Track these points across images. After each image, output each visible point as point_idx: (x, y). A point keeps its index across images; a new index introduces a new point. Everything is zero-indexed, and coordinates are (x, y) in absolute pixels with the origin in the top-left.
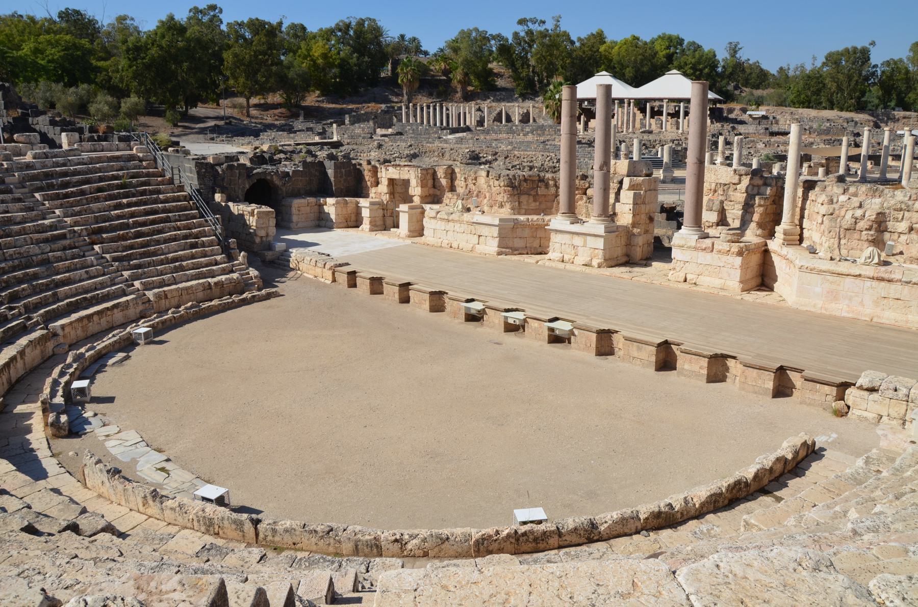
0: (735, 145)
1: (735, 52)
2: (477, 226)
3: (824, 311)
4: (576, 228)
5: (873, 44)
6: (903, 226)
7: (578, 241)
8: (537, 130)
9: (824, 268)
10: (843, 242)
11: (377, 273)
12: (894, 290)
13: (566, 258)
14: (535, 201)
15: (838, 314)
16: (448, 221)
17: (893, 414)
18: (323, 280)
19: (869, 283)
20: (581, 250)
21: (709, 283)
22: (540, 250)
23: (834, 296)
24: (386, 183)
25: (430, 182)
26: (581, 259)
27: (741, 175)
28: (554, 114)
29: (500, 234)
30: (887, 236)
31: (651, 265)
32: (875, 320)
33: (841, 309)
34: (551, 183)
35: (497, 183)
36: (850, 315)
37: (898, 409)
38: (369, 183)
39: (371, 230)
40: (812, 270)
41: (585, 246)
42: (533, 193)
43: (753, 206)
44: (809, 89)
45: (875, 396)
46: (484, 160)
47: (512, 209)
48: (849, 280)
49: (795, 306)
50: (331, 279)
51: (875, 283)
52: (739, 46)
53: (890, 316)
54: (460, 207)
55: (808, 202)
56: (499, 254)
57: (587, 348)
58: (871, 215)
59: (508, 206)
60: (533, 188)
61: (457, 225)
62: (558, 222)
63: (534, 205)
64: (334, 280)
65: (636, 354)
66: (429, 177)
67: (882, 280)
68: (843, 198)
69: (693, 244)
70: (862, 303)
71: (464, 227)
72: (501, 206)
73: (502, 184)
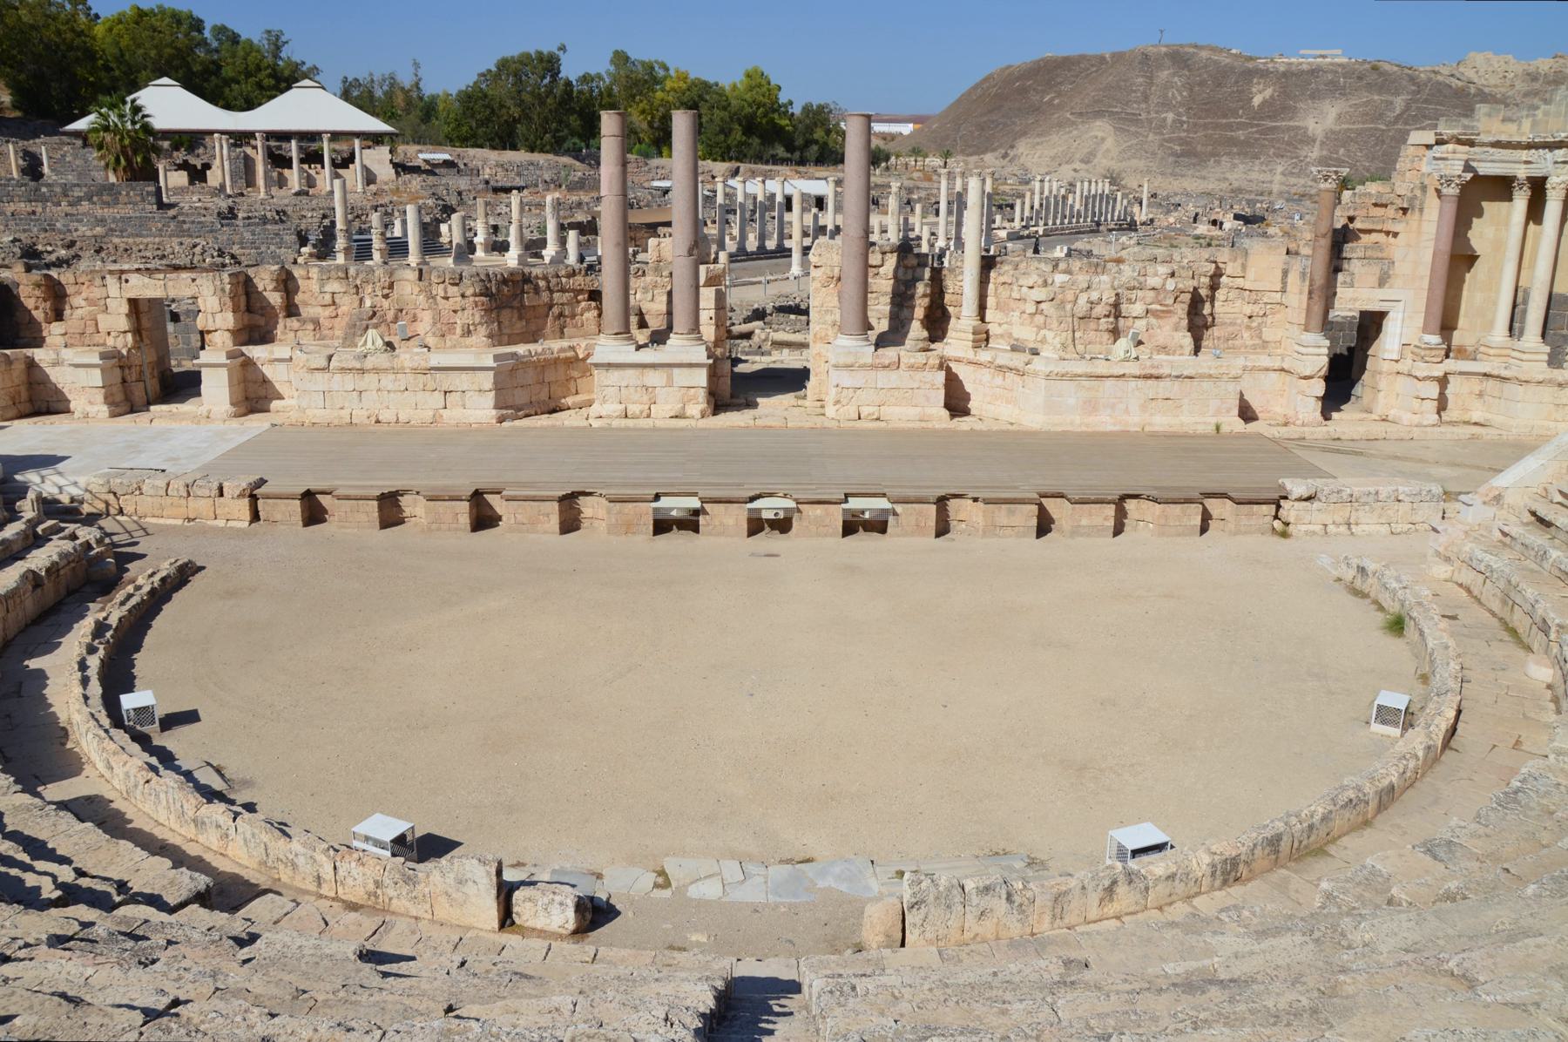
0: (548, 209)
1: (278, 48)
2: (439, 375)
3: (1084, 429)
4: (648, 356)
5: (563, 48)
6: (1138, 309)
7: (655, 378)
8: (99, 194)
9: (1079, 371)
10: (1077, 335)
11: (389, 485)
12: (1162, 388)
13: (634, 409)
14: (520, 318)
15: (1102, 429)
16: (362, 371)
17: (1339, 519)
18: (221, 523)
19: (1133, 384)
20: (661, 394)
21: (902, 415)
22: (552, 405)
23: (1091, 406)
24: (125, 308)
25: (243, 299)
26: (662, 411)
27: (884, 253)
28: (117, 160)
29: (495, 383)
30: (1121, 321)
31: (754, 405)
32: (1147, 429)
33: (1105, 422)
34: (542, 283)
35: (453, 290)
36: (1117, 428)
37: (1341, 513)
38: (38, 315)
39: (113, 415)
40: (1062, 376)
41: (670, 384)
42: (516, 304)
43: (912, 297)
44: (472, 116)
45: (1316, 505)
46: (53, 257)
47: (490, 336)
48: (1109, 383)
49: (1046, 428)
50: (247, 515)
51: (1141, 383)
52: (284, 39)
53: (1161, 421)
54: (379, 343)
55: (991, 286)
56: (501, 420)
57: (919, 530)
58: (1109, 297)
59: (483, 330)
60: (515, 296)
61: (387, 381)
62: (608, 348)
63: (519, 326)
64: (255, 516)
65: (1005, 522)
66: (241, 290)
67: (1150, 377)
68: (1060, 278)
69: (869, 361)
70: (1127, 411)
71: (403, 380)
72: (468, 332)
73: (469, 292)
